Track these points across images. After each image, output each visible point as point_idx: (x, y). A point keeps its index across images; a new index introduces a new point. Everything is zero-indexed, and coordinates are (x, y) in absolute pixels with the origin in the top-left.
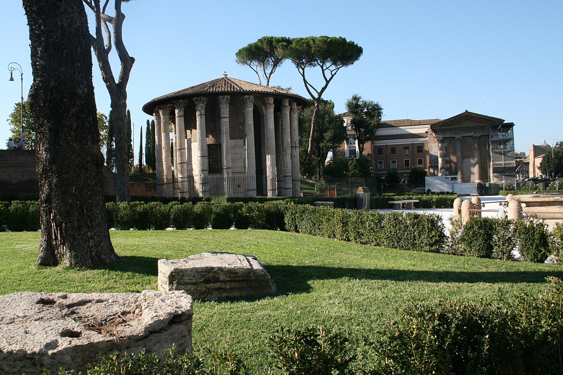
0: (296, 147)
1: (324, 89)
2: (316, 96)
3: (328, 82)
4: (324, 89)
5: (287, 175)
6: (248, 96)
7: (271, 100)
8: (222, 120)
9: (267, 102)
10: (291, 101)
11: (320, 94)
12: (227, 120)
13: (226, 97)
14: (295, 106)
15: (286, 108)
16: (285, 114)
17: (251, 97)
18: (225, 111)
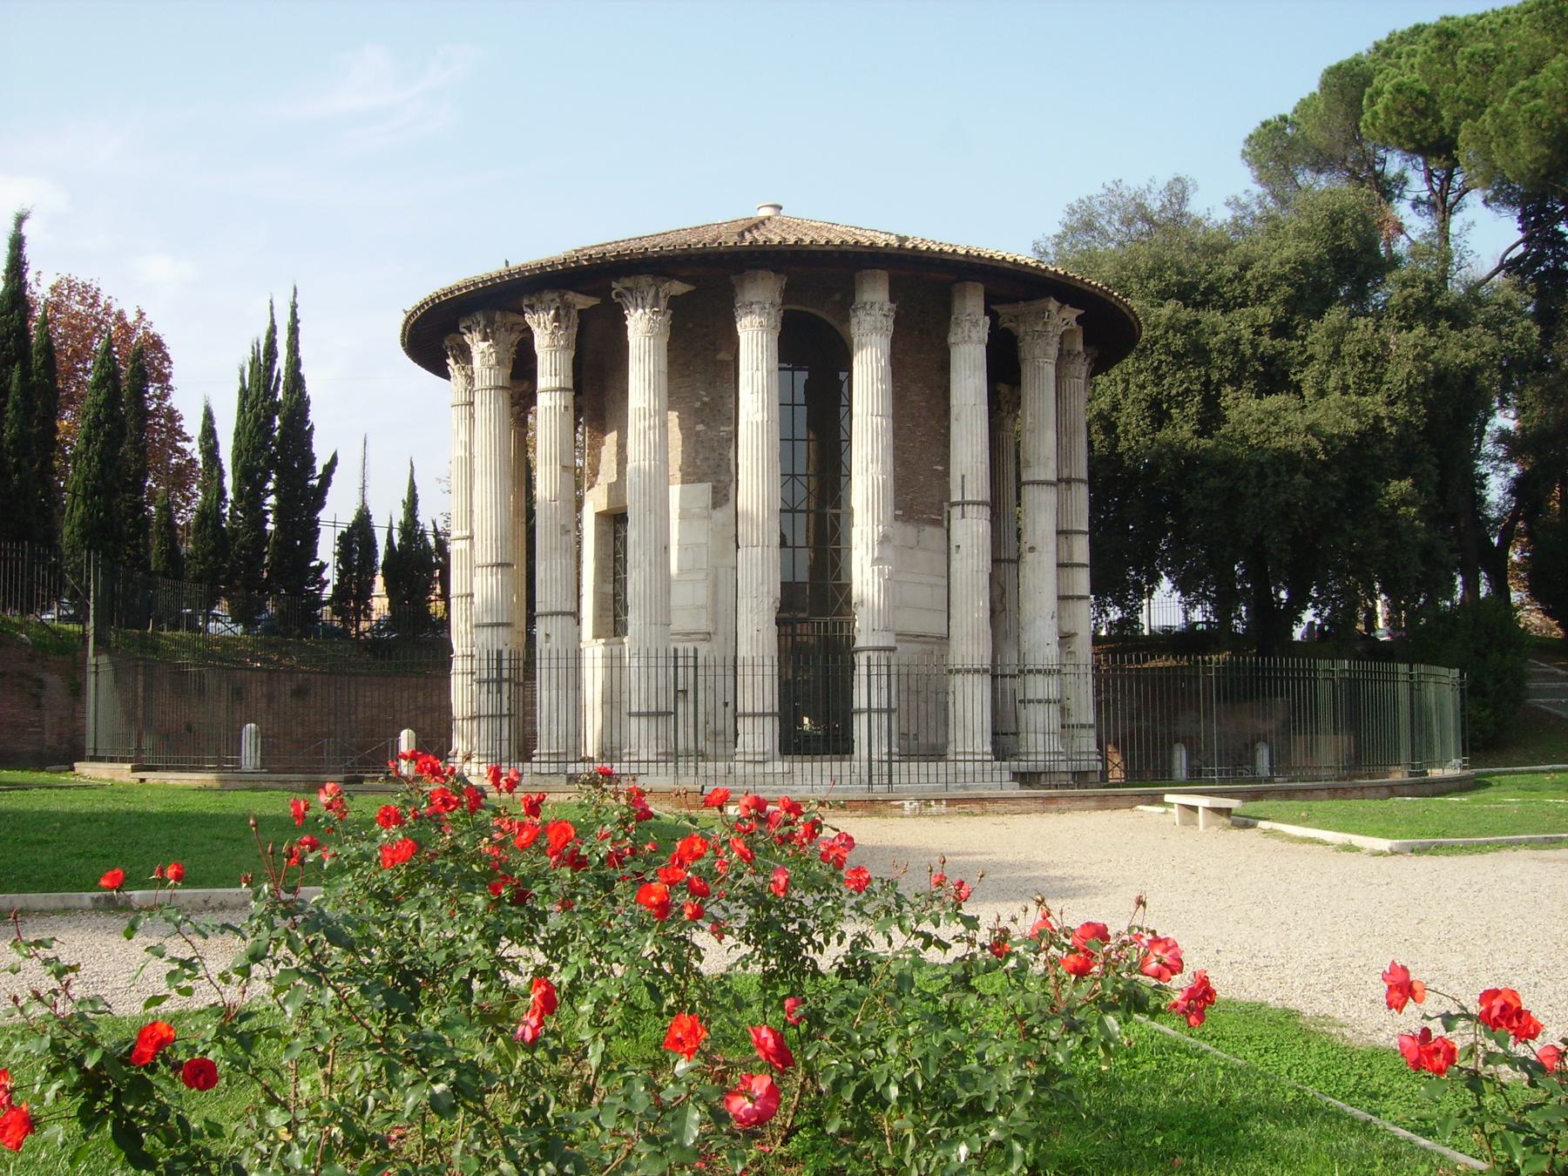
6: (628, 283)
13: (548, 296)
15: (861, 314)
17: (644, 280)
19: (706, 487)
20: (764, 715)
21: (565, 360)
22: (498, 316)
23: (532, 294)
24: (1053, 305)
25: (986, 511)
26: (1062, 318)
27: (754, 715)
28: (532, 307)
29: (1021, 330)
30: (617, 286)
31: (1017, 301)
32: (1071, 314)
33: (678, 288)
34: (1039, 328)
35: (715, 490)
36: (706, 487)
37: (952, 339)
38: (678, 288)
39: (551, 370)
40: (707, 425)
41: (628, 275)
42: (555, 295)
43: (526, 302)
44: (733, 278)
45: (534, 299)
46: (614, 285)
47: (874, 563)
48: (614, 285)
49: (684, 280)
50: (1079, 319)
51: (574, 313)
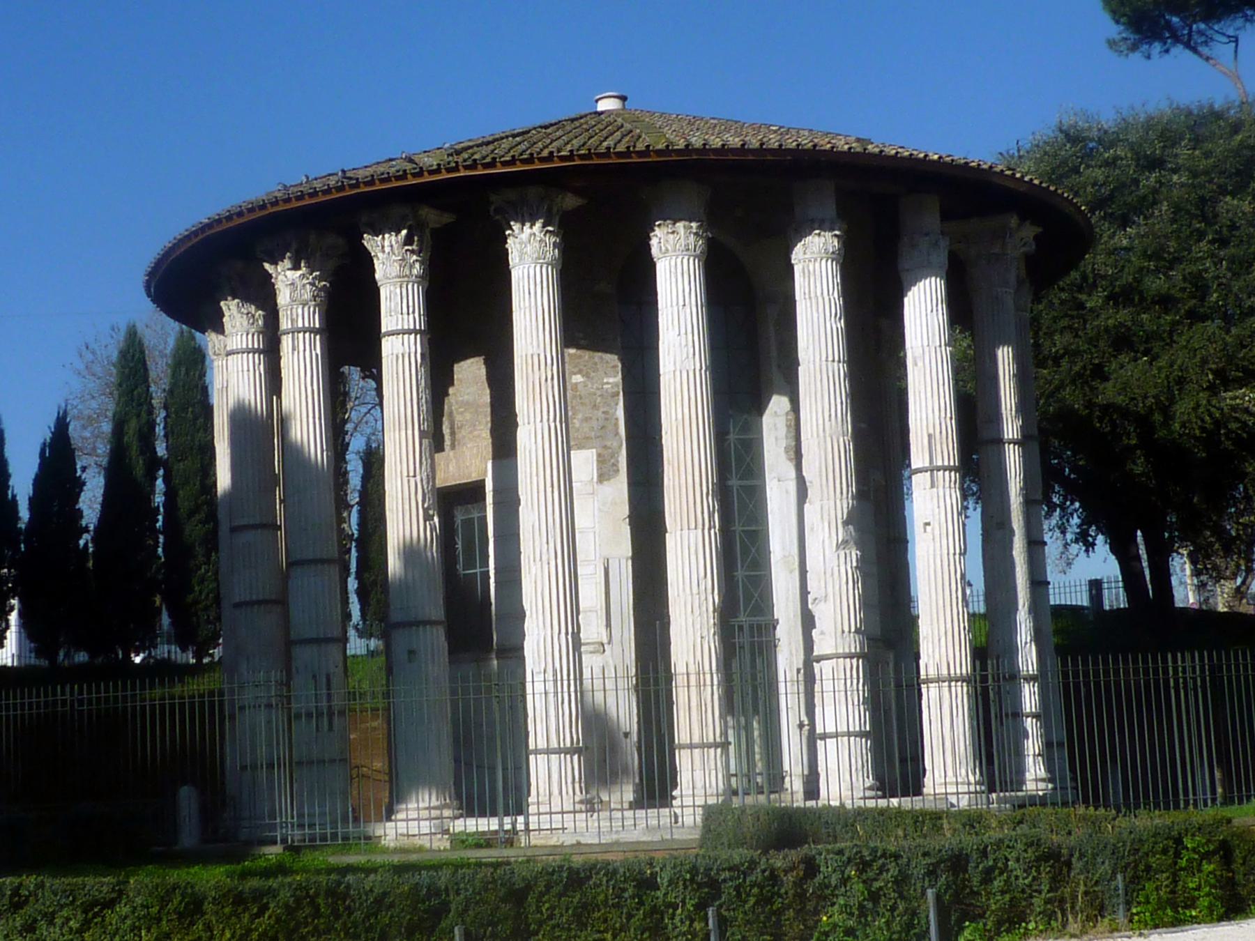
8: (389, 347)
20: (703, 746)
21: (415, 294)
24: (1014, 221)
26: (1023, 236)
27: (836, 735)
32: (1029, 232)
33: (571, 201)
34: (996, 250)
35: (601, 460)
38: (571, 201)
39: (400, 305)
40: (587, 376)
46: (493, 198)
47: (838, 547)
48: (493, 198)
49: (577, 192)
50: (1036, 238)
51: (428, 232)
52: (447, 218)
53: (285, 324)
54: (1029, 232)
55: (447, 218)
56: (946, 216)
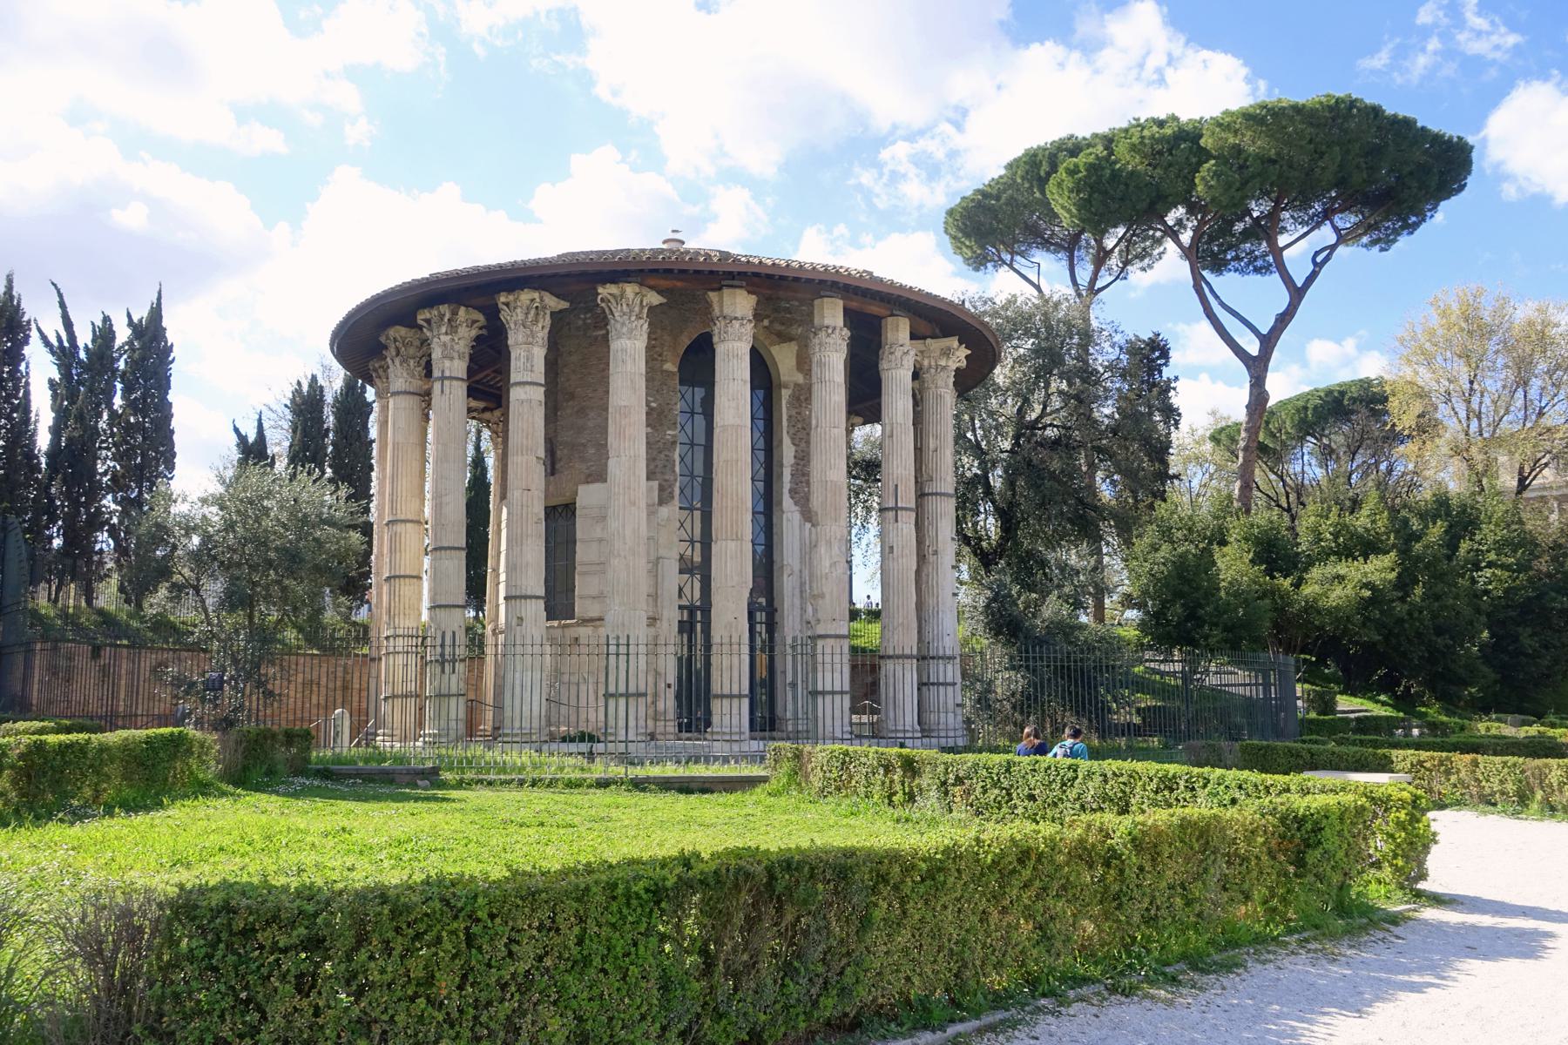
0: (896, 509)
1: (1284, 319)
2: (1253, 348)
3: (1297, 294)
4: (1284, 319)
5: (820, 630)
7: (740, 304)
8: (516, 394)
9: (717, 312)
10: (875, 309)
11: (1268, 342)
12: (539, 394)
13: (526, 296)
14: (898, 331)
15: (823, 334)
16: (821, 364)
17: (630, 290)
18: (528, 360)
19: (655, 484)
22: (462, 310)
23: (510, 290)
24: (953, 342)
25: (913, 515)
26: (960, 356)
28: (507, 304)
29: (926, 363)
30: (605, 291)
31: (924, 338)
32: (963, 352)
34: (943, 363)
35: (661, 489)
36: (655, 484)
37: (883, 365)
38: (654, 299)
41: (613, 282)
42: (536, 295)
43: (503, 299)
44: (711, 294)
45: (511, 298)
49: (660, 292)
52: (564, 305)
53: (436, 373)
54: (963, 352)
55: (564, 305)
56: (913, 337)
